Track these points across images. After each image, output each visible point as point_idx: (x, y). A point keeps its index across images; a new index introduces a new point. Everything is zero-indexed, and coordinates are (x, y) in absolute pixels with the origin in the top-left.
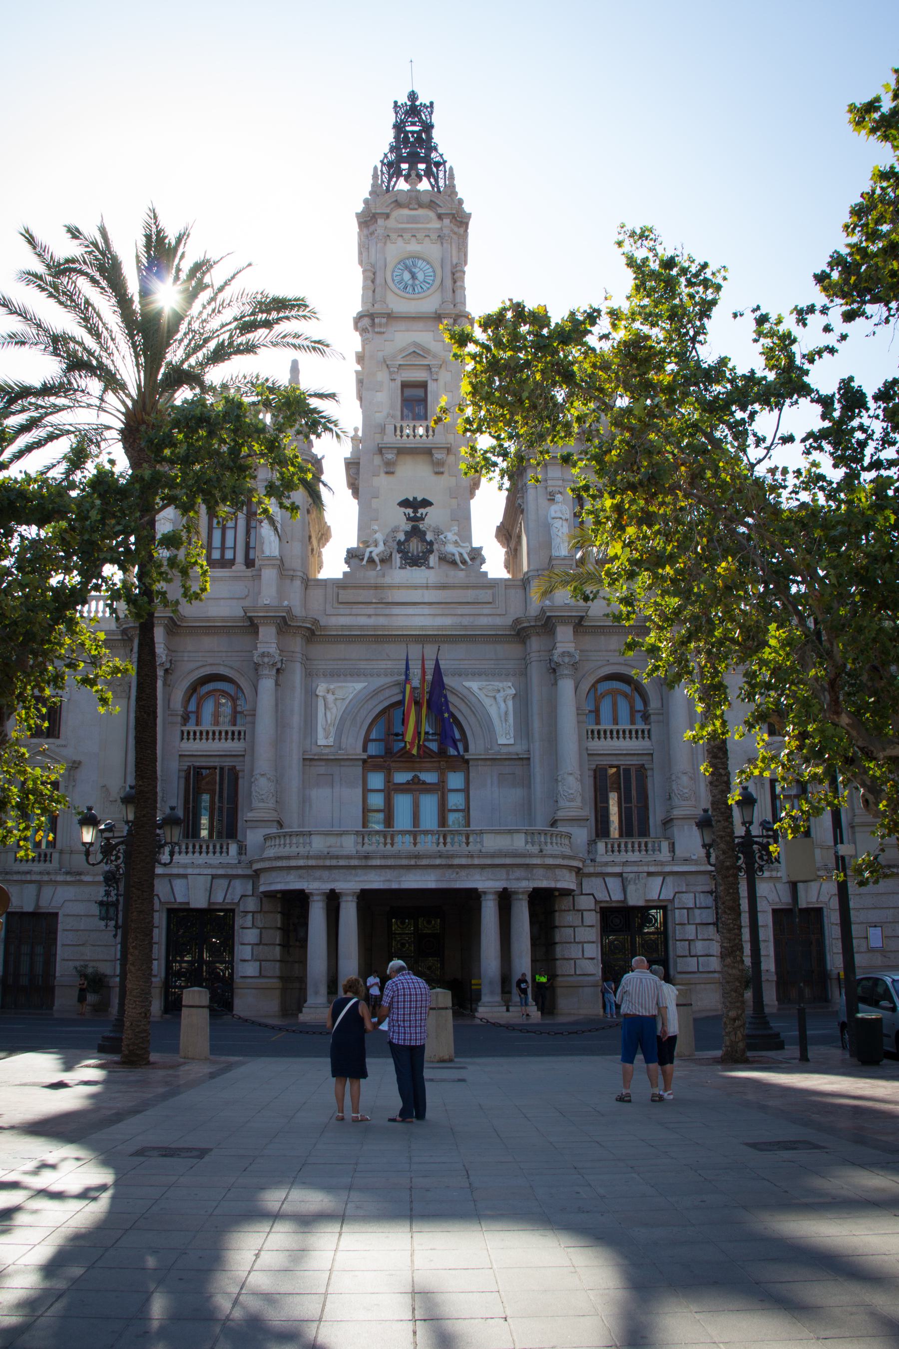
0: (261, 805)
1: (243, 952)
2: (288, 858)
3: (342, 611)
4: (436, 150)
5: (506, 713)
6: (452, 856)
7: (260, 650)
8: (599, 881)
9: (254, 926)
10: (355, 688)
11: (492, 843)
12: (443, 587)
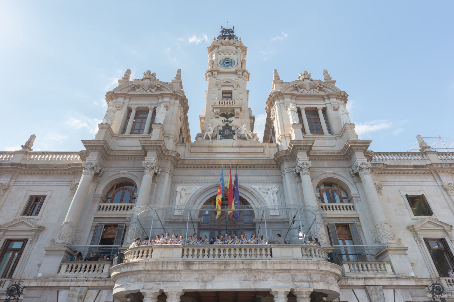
3: (192, 156)
5: (274, 200)
8: (350, 291)
10: (195, 188)
12: (240, 146)
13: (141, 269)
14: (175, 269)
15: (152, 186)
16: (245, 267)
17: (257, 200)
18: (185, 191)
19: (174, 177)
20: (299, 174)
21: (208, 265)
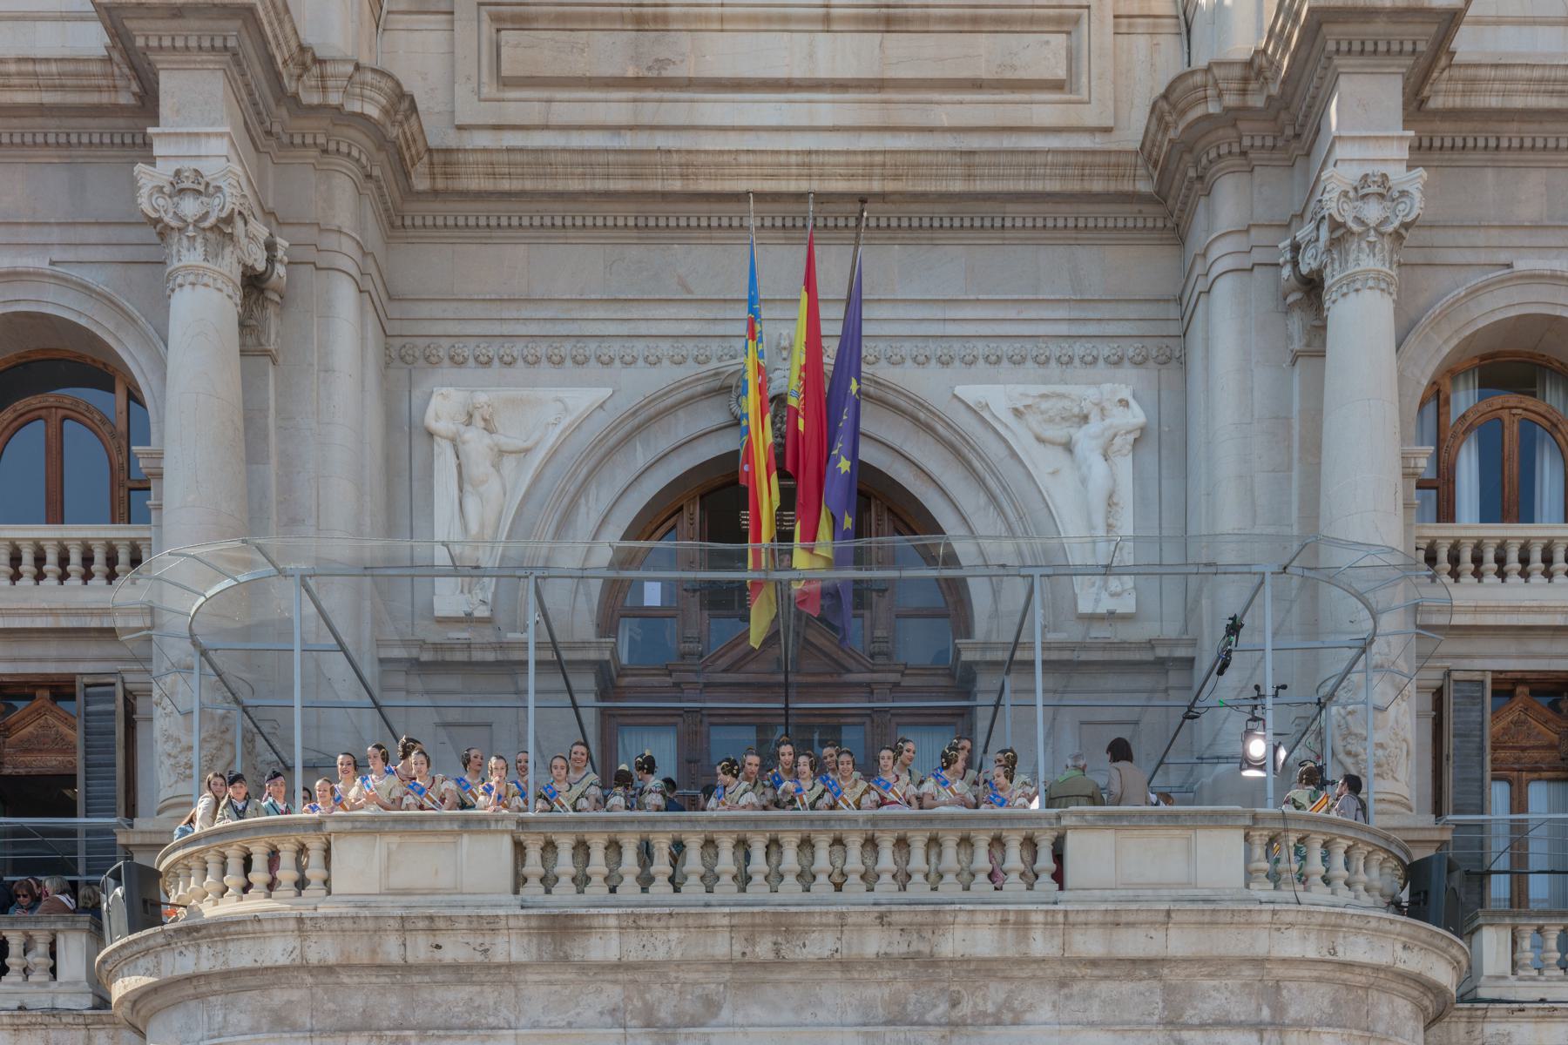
5: (1111, 502)
13: (283, 960)
14: (479, 958)
15: (250, 385)
16: (899, 948)
17: (993, 498)
18: (489, 428)
19: (394, 310)
20: (1312, 287)
21: (674, 935)
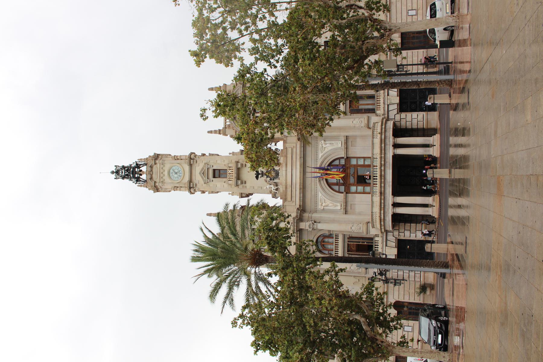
0: (361, 229)
1: (413, 237)
2: (381, 220)
3: (294, 200)
4: (131, 165)
6: (381, 164)
7: (308, 228)
9: (404, 233)
11: (377, 150)
12: (286, 165)
